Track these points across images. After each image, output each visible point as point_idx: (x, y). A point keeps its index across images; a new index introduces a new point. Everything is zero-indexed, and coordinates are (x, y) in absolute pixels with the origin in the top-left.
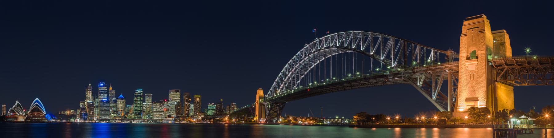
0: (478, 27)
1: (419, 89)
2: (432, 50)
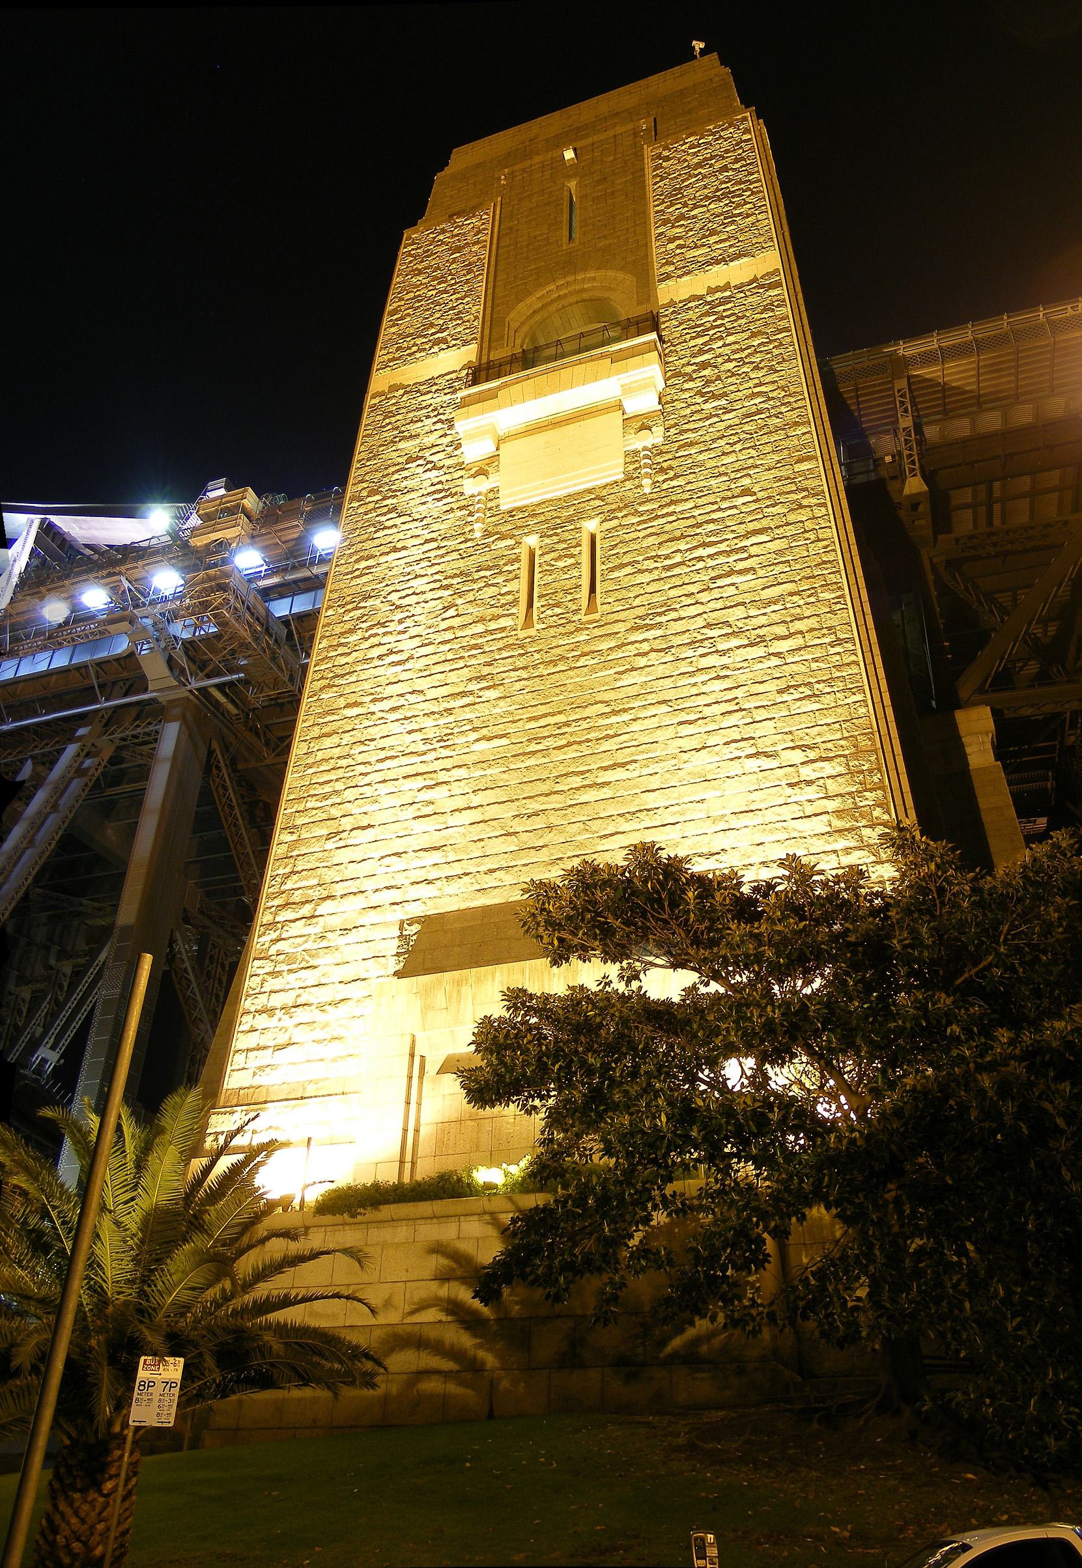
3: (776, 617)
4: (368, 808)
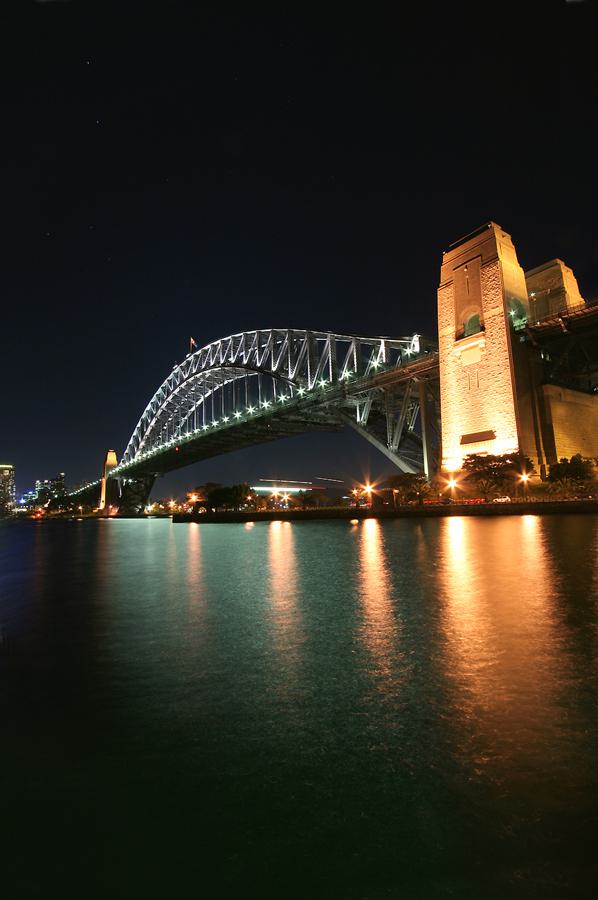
1: (360, 431)
2: (383, 341)
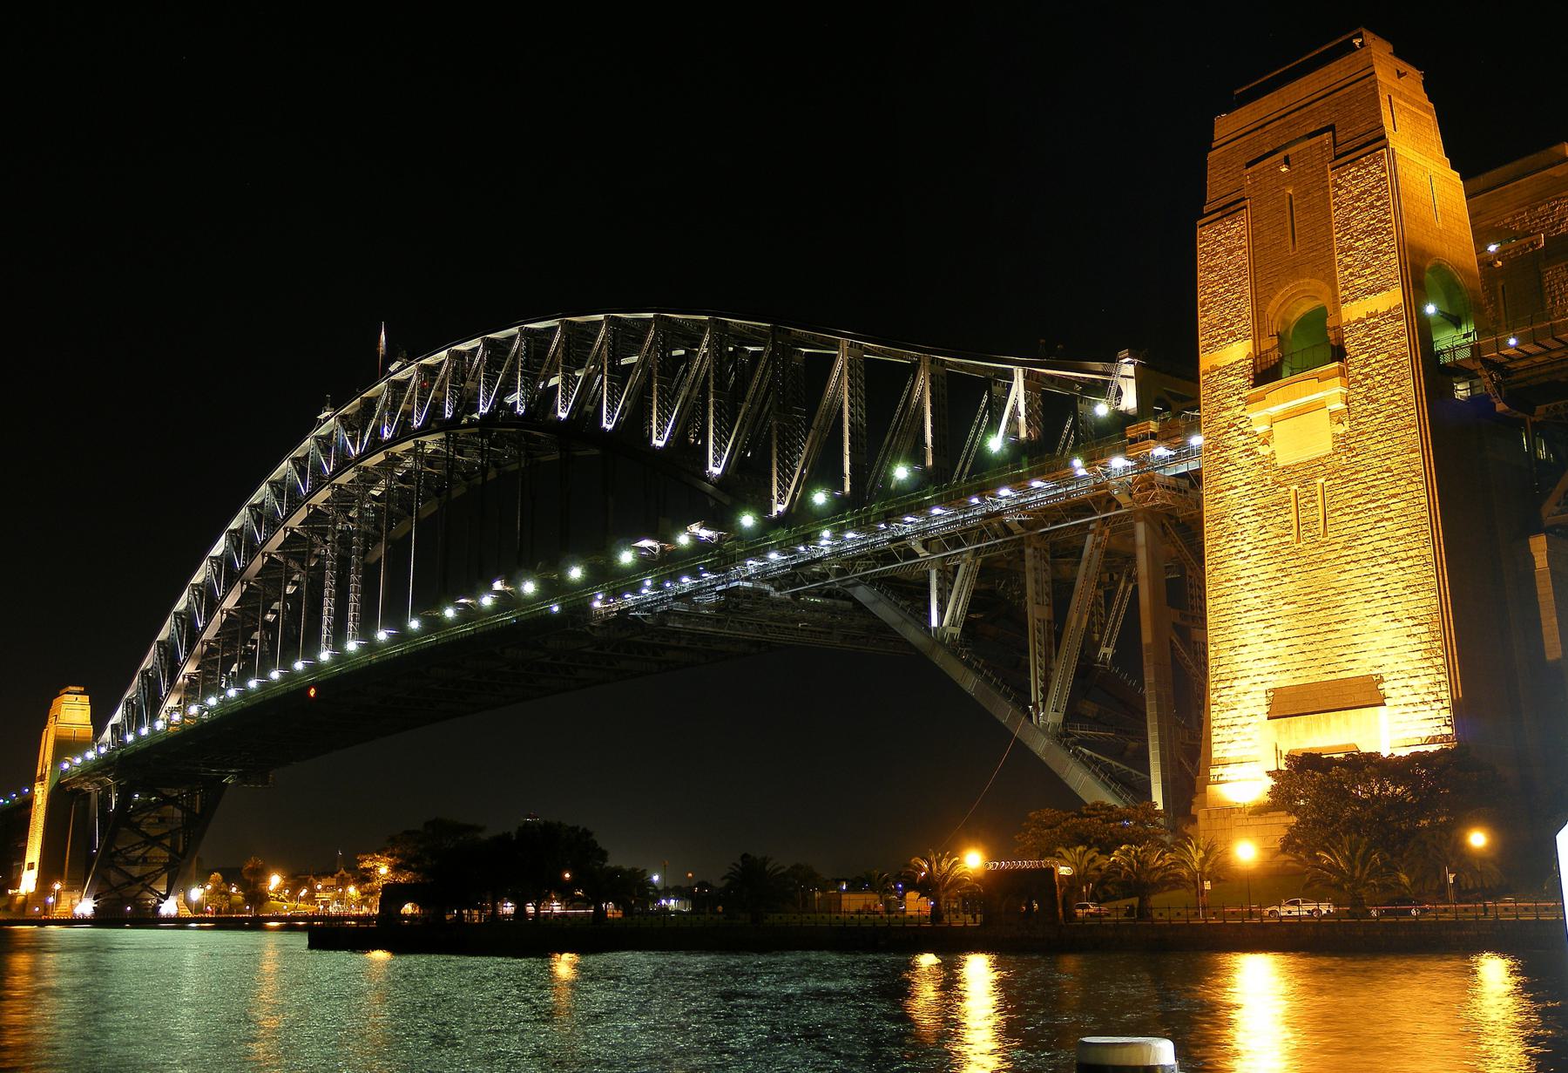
0: (1331, 128)
1: (940, 658)
2: (1019, 374)
3: (1402, 547)
4: (1245, 636)
